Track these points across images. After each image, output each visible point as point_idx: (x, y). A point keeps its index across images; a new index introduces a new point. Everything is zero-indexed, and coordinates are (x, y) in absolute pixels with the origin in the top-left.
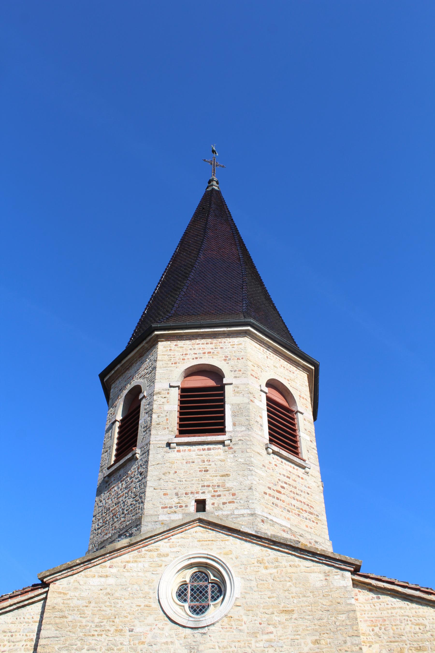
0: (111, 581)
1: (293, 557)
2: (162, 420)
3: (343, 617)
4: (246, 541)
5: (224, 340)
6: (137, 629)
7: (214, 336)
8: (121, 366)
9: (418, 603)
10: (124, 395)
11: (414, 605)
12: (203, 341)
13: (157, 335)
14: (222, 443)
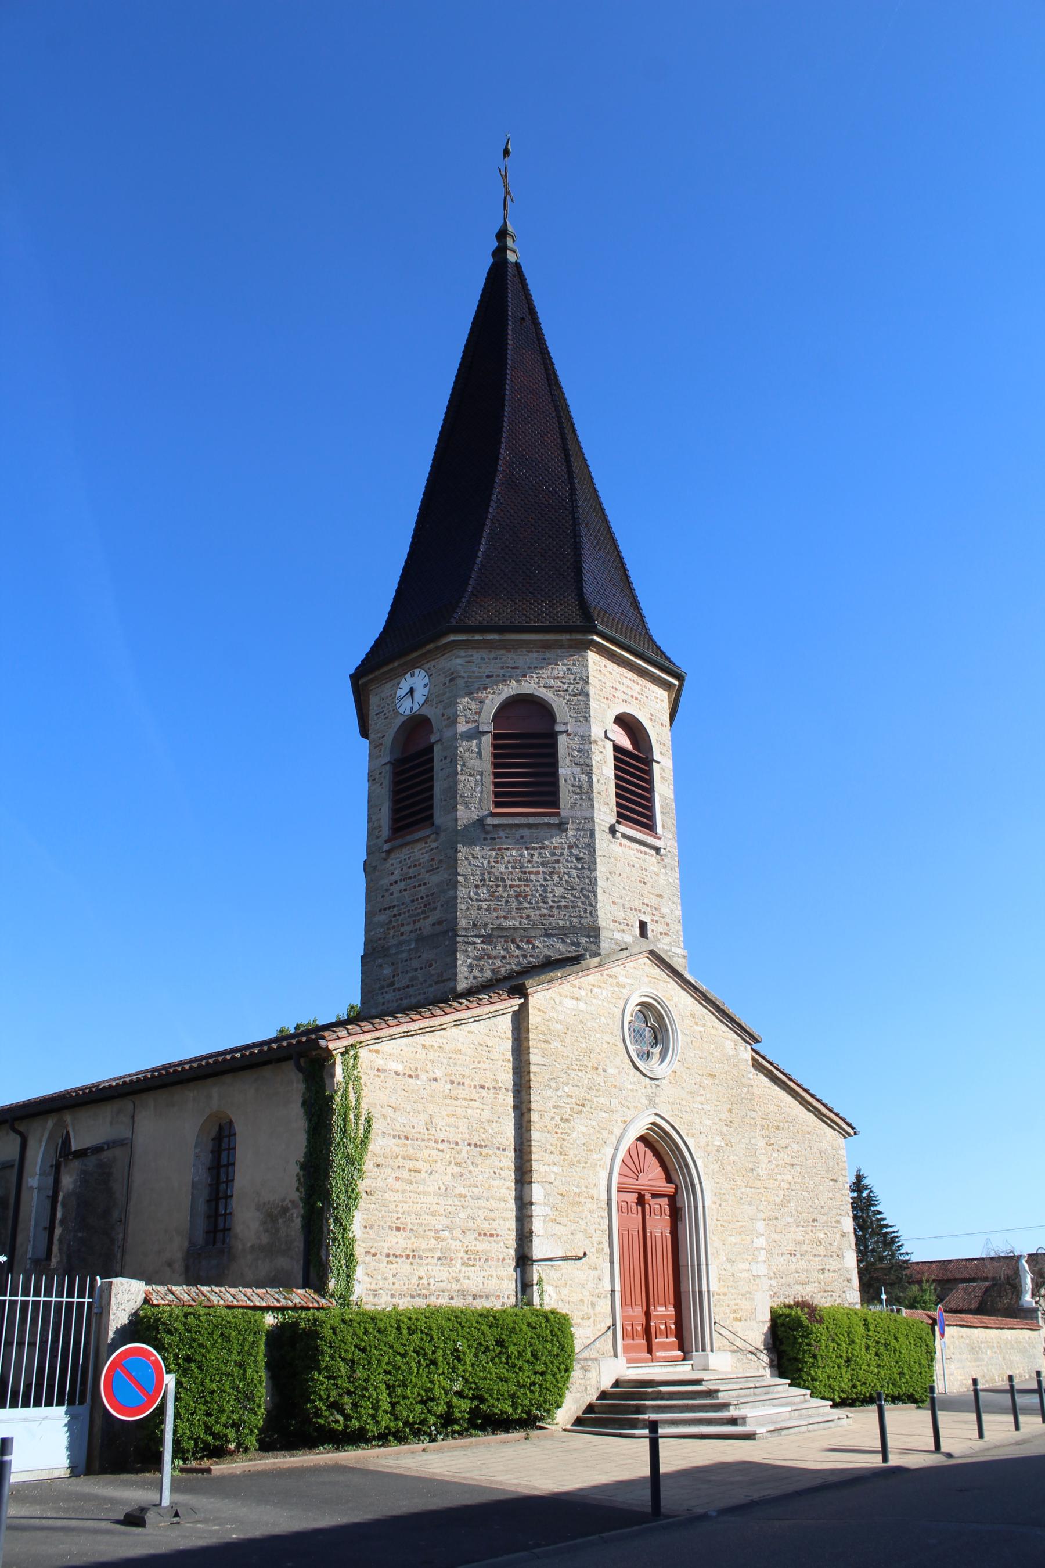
0: (582, 1006)
1: (714, 1018)
2: (602, 788)
3: (745, 1090)
4: (682, 988)
5: (649, 685)
6: (610, 1071)
7: (642, 673)
8: (500, 641)
9: (779, 1086)
10: (504, 696)
11: (776, 1088)
12: (630, 675)
13: (593, 640)
14: (657, 850)
